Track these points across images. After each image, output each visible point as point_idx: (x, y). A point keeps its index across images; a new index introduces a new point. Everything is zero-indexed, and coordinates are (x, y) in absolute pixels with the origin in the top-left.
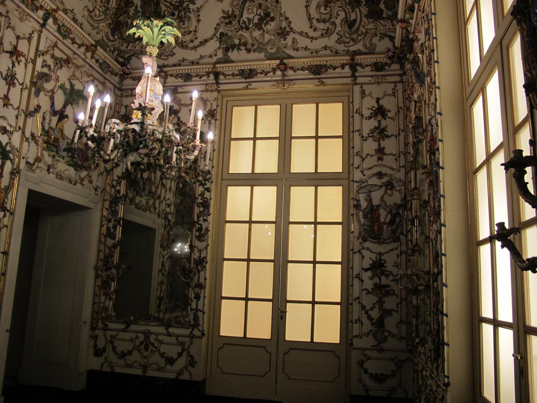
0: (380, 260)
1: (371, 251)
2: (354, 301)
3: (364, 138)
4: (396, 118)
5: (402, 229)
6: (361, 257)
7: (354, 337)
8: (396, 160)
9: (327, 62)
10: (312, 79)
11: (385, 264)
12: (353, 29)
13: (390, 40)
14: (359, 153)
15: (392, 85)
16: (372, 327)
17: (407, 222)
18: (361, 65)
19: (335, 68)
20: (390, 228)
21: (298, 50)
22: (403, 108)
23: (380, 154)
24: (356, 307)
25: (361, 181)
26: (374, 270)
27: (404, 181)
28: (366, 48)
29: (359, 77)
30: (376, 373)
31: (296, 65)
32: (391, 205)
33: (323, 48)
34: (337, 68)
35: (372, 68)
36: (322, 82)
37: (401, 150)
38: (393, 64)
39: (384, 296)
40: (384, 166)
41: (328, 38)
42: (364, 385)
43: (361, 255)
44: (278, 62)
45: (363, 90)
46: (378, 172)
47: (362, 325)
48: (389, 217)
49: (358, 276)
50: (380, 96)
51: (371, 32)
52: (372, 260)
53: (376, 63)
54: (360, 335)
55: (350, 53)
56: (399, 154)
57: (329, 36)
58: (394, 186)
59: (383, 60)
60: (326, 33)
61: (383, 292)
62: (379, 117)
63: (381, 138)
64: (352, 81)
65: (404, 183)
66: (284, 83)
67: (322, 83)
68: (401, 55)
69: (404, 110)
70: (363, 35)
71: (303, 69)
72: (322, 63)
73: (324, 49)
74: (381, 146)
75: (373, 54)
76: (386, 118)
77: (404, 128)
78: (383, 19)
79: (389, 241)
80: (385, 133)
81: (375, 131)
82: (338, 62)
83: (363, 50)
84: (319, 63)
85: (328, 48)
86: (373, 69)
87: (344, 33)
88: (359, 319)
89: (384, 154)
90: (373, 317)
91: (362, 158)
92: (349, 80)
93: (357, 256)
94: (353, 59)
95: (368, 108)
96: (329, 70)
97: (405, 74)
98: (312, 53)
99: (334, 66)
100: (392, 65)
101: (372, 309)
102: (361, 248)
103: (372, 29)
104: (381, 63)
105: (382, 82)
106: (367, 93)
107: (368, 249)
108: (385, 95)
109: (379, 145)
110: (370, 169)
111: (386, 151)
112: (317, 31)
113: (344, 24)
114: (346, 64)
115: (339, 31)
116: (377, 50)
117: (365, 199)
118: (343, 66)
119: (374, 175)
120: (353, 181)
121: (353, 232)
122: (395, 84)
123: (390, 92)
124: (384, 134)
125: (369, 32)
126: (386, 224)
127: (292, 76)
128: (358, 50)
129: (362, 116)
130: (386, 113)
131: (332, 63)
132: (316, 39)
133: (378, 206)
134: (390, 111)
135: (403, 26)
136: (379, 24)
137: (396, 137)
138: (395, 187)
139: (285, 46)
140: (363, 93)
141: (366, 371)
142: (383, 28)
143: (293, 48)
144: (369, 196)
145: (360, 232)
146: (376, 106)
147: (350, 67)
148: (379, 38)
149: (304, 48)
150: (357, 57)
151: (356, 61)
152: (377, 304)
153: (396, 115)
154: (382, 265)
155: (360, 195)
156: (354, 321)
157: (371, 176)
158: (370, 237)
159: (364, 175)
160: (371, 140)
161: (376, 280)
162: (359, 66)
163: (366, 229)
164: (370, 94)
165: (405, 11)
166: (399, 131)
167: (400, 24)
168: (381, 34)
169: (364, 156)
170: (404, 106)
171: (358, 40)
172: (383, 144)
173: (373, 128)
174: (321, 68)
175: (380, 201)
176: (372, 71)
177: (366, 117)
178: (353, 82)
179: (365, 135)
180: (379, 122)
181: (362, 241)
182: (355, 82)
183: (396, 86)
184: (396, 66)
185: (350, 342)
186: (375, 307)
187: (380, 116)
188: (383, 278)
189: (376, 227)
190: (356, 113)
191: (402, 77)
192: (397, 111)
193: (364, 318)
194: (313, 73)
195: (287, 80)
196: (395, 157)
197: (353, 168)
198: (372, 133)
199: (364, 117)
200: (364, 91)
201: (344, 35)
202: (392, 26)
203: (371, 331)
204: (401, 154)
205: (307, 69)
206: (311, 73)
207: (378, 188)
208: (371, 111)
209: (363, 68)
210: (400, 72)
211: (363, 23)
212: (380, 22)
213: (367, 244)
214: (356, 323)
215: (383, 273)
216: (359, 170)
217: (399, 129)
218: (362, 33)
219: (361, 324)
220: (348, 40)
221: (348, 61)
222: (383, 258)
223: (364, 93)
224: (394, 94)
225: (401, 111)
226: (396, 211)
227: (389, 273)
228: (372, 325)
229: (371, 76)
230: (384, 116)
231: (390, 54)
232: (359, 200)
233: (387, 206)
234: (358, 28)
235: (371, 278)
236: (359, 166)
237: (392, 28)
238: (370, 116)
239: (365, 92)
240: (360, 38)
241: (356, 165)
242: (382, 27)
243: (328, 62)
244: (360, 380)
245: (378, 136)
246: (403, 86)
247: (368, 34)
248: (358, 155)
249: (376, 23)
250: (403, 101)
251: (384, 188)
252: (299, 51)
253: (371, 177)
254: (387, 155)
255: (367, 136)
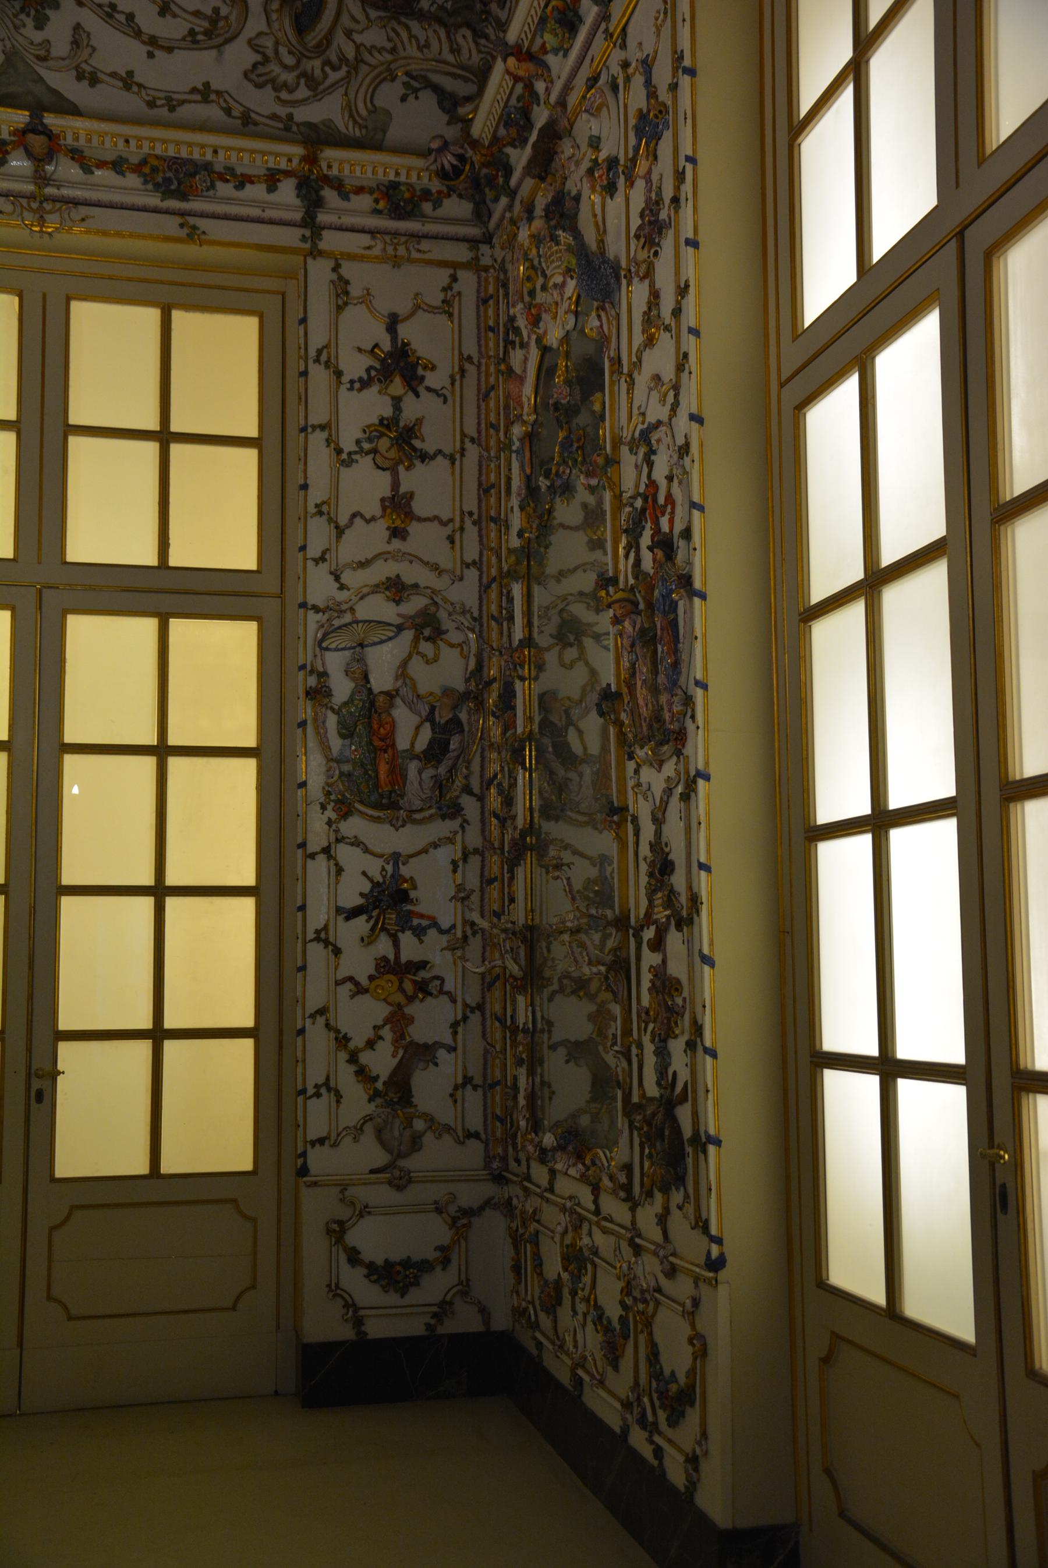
0: (397, 877)
1: (366, 850)
2: (308, 1021)
3: (344, 456)
4: (453, 393)
5: (466, 777)
6: (333, 869)
7: (313, 1143)
8: (451, 540)
9: (215, 152)
10: (156, 210)
11: (413, 894)
12: (313, 38)
13: (440, 104)
14: (325, 508)
15: (443, 276)
16: (373, 1105)
17: (483, 750)
18: (338, 185)
19: (243, 181)
20: (429, 772)
21: (94, 80)
22: (475, 361)
23: (399, 516)
24: (318, 1038)
25: (333, 609)
26: (375, 913)
27: (476, 614)
28: (355, 122)
29: (330, 228)
30: (386, 1261)
31: (95, 142)
32: (431, 694)
33: (194, 90)
34: (252, 183)
35: (377, 201)
36: (194, 228)
37: (466, 509)
38: (449, 196)
39: (411, 999)
40: (412, 558)
41: (213, 53)
42: (346, 1306)
43: (332, 862)
44: (21, 117)
45: (341, 278)
46: (388, 579)
47: (338, 1102)
48: (426, 734)
49: (322, 937)
50: (402, 310)
51: (373, 62)
52: (371, 880)
53: (394, 186)
54: (333, 1136)
55: (295, 128)
56: (462, 521)
57: (219, 47)
58: (444, 628)
59: (419, 177)
60: (208, 33)
61: (408, 986)
62: (397, 386)
63: (401, 462)
64: (304, 239)
65: (474, 619)
66: (41, 207)
67: (193, 235)
68: (484, 171)
69: (479, 367)
70: (345, 69)
71: (118, 165)
72: (196, 156)
73: (198, 97)
74: (402, 490)
75: (378, 147)
76: (421, 390)
77: (479, 432)
78: (422, 16)
79: (427, 814)
80: (417, 443)
81: (382, 435)
82: (259, 162)
83: (343, 130)
84: (184, 154)
85: (213, 97)
86: (381, 205)
87: (277, 43)
88: (327, 1084)
89: (410, 515)
90: (374, 1074)
91: (337, 527)
92: (291, 237)
93: (320, 867)
94: (311, 160)
95: (360, 350)
96: (219, 185)
97: (488, 239)
98: (151, 104)
99: (239, 171)
100: (446, 202)
101: (371, 1044)
102: (332, 839)
103: (379, 51)
104: (410, 187)
105: (409, 260)
106: (355, 291)
107: (356, 843)
108: (417, 307)
109: (396, 484)
110: (363, 565)
111: (419, 507)
112: (175, 16)
113: (279, 10)
114: (288, 174)
115: (260, 34)
116: (395, 134)
117: (347, 672)
118: (272, 179)
119: (376, 589)
120: (303, 605)
121: (303, 785)
122: (452, 271)
123: (435, 298)
124: (414, 449)
125: (366, 56)
126: (417, 757)
127: (73, 185)
128: (323, 122)
129: (339, 374)
130: (420, 371)
131: (234, 159)
132: (170, 50)
133: (390, 696)
134: (433, 368)
135: (521, 73)
136: (404, 35)
137: (452, 460)
138: (448, 631)
139: (42, 53)
140: (341, 288)
141: (354, 1257)
142: (419, 55)
143: (77, 68)
144: (361, 660)
145: (328, 785)
146: (386, 345)
147: (299, 187)
148: (402, 91)
149: (122, 79)
150: (329, 154)
151: (324, 165)
152: (388, 1027)
153: (453, 384)
154: (403, 897)
155: (327, 654)
156: (311, 1091)
157: (365, 590)
158: (361, 802)
159: (342, 587)
160: (366, 462)
161: (383, 946)
162: (332, 187)
163: (349, 775)
164: (367, 298)
165: (543, 20)
166: (462, 442)
167: (512, 61)
168: (407, 74)
169: (343, 521)
170: (480, 352)
171: (327, 83)
172: (409, 480)
173: (377, 422)
174: (193, 175)
175: (397, 678)
176: (377, 212)
177: (352, 382)
178: (308, 246)
179: (348, 444)
180: (397, 402)
181: (334, 816)
182: (314, 245)
183: (454, 279)
184: (457, 207)
185: (300, 1161)
186: (381, 1038)
187: (398, 380)
188: (407, 939)
189: (383, 769)
190: (317, 360)
191: (478, 249)
192: (457, 369)
193: (346, 1077)
194: (157, 186)
195: (55, 200)
196: (447, 530)
197: (305, 559)
198: (370, 440)
199: (345, 379)
200: (347, 282)
201: (276, 52)
202: (452, 51)
203: (368, 1119)
204: (468, 522)
205: (138, 169)
206: (150, 186)
207: (391, 634)
208: (367, 361)
209: (345, 196)
210: (474, 231)
211: (346, 21)
212: (408, 28)
213: (353, 826)
214: (318, 1095)
215: (405, 922)
216: (324, 567)
217: (463, 435)
218: (343, 59)
219: (333, 1099)
220: (289, 77)
221: (295, 162)
222: (404, 870)
223: (347, 293)
224: (447, 307)
225: (471, 370)
226: (451, 716)
227: (425, 923)
228: (371, 1100)
229: (372, 233)
230: (414, 383)
231: (448, 160)
232: (323, 675)
233: (418, 696)
234: (329, 37)
235: (367, 941)
236: (324, 553)
237: (450, 58)
238: (365, 377)
239: (349, 288)
240: (333, 76)
241: (314, 551)
242: (412, 51)
243: (221, 153)
244: (334, 1290)
245: (393, 454)
246: (479, 283)
247: (364, 69)
248: (320, 513)
249: (394, 30)
250: (479, 338)
251: (408, 635)
252: (98, 86)
253: (368, 594)
254: (420, 520)
255: (355, 448)
